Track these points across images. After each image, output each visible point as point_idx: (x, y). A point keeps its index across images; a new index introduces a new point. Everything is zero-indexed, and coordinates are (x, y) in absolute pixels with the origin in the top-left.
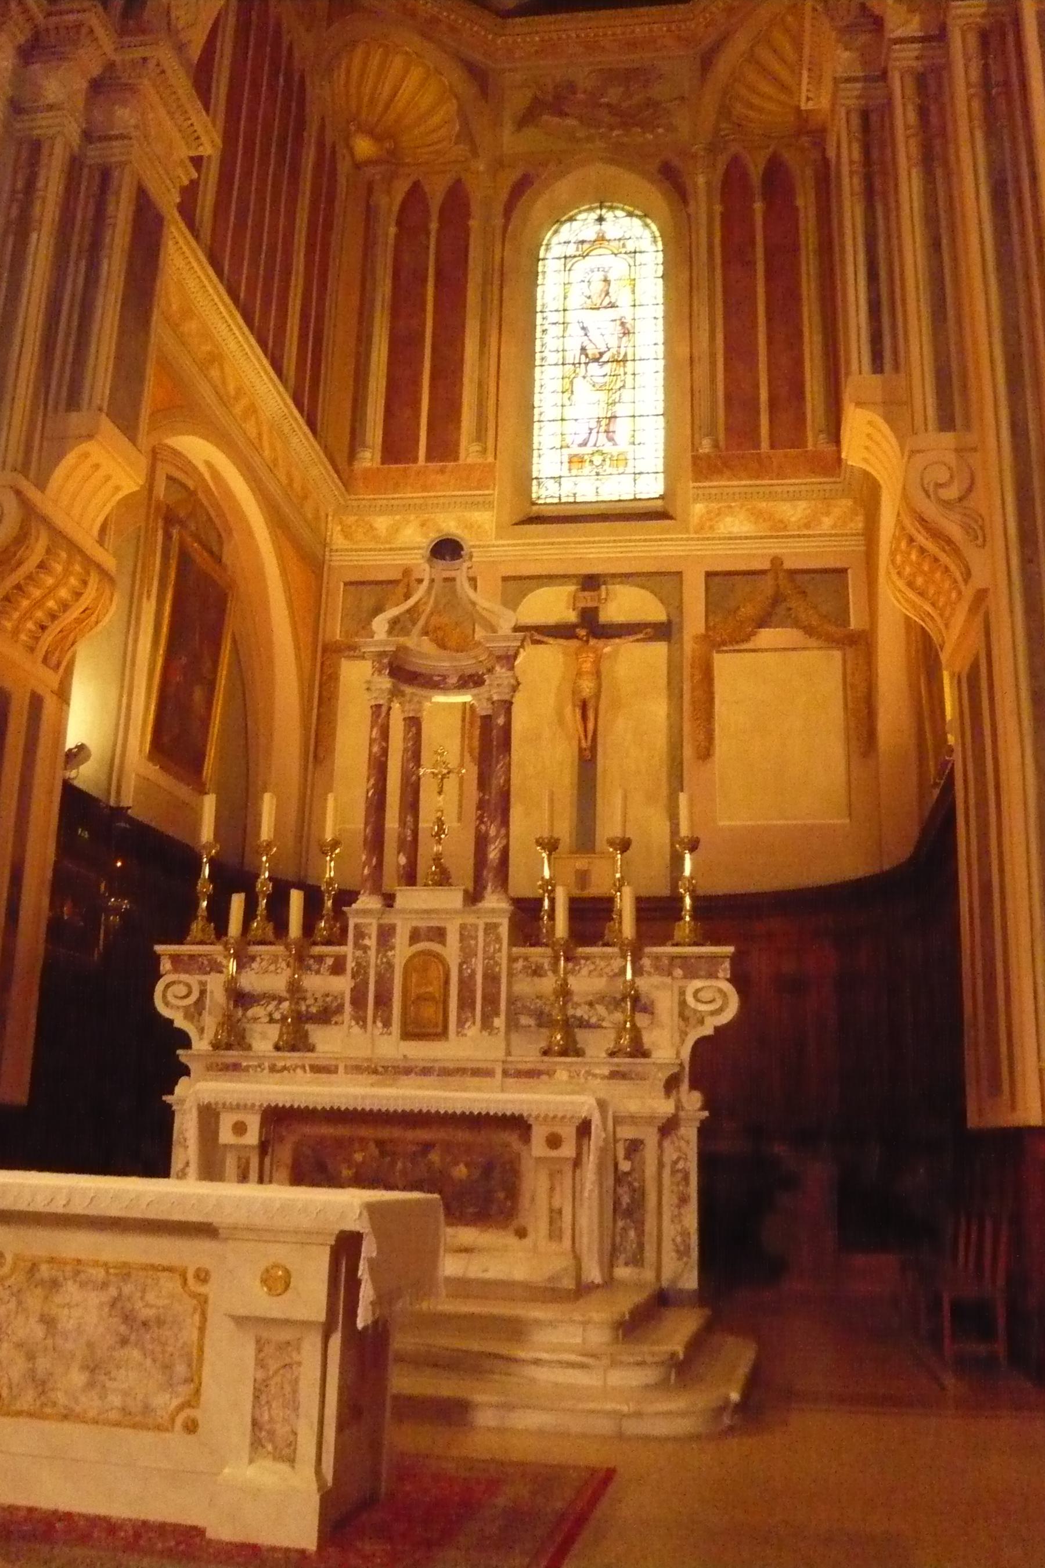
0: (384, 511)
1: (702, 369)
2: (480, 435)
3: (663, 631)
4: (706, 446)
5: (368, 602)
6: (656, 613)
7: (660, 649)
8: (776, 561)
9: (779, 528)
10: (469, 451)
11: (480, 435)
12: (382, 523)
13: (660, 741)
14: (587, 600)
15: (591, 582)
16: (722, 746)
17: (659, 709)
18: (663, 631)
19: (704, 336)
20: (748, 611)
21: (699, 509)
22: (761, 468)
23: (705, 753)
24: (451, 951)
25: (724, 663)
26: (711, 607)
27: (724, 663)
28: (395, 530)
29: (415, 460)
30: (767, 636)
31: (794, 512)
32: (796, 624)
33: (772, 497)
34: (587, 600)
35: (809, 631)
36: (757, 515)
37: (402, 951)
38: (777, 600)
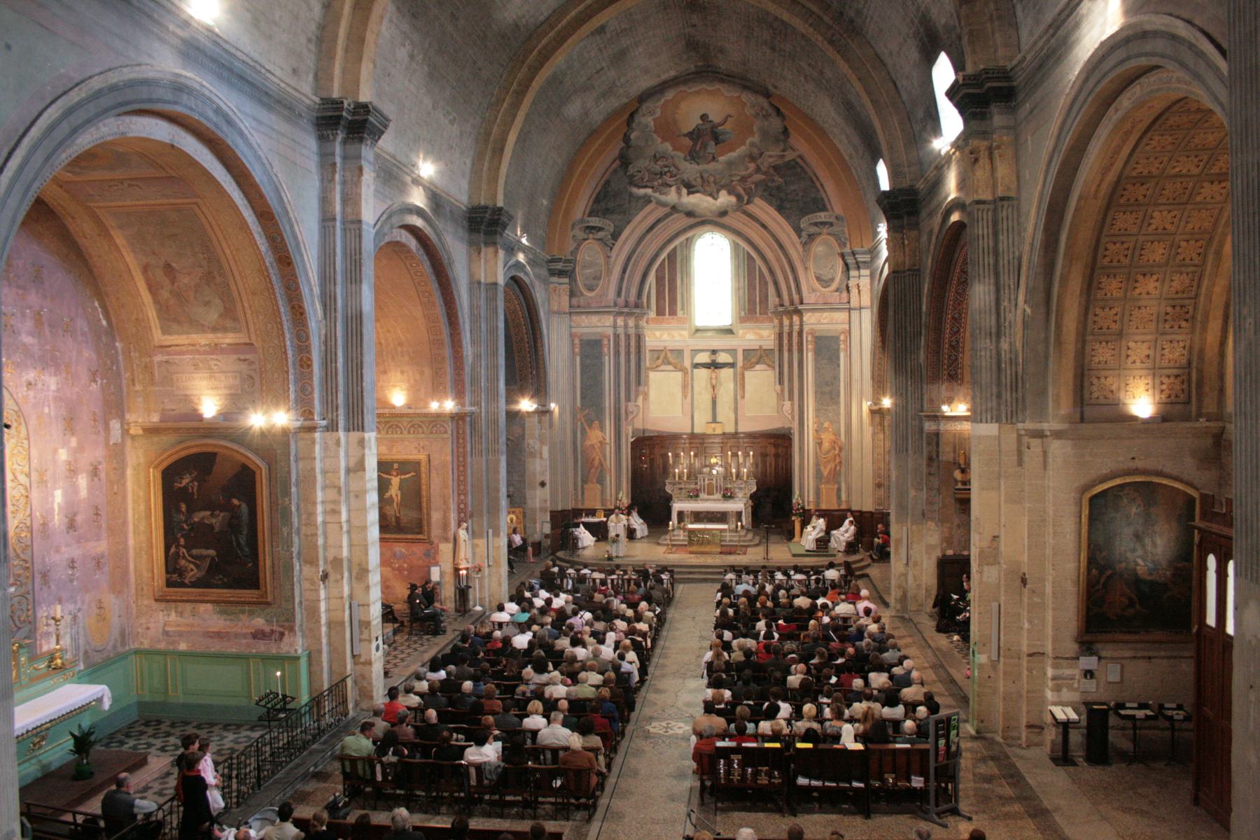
0: (658, 330)
1: (741, 291)
2: (683, 309)
3: (732, 365)
4: (743, 314)
5: (656, 356)
6: (730, 360)
7: (732, 370)
8: (760, 347)
9: (761, 337)
10: (680, 313)
11: (683, 309)
12: (658, 333)
13: (732, 394)
14: (713, 357)
15: (714, 352)
16: (747, 395)
17: (732, 386)
18: (732, 365)
19: (742, 280)
20: (754, 360)
21: (741, 332)
22: (757, 321)
23: (743, 397)
24: (714, 482)
25: (748, 374)
26: (745, 358)
27: (748, 374)
28: (662, 335)
29: (664, 315)
30: (758, 367)
31: (765, 333)
32: (765, 363)
33: (760, 328)
34: (713, 357)
35: (769, 366)
36: (756, 334)
37: (707, 482)
38: (761, 357)
